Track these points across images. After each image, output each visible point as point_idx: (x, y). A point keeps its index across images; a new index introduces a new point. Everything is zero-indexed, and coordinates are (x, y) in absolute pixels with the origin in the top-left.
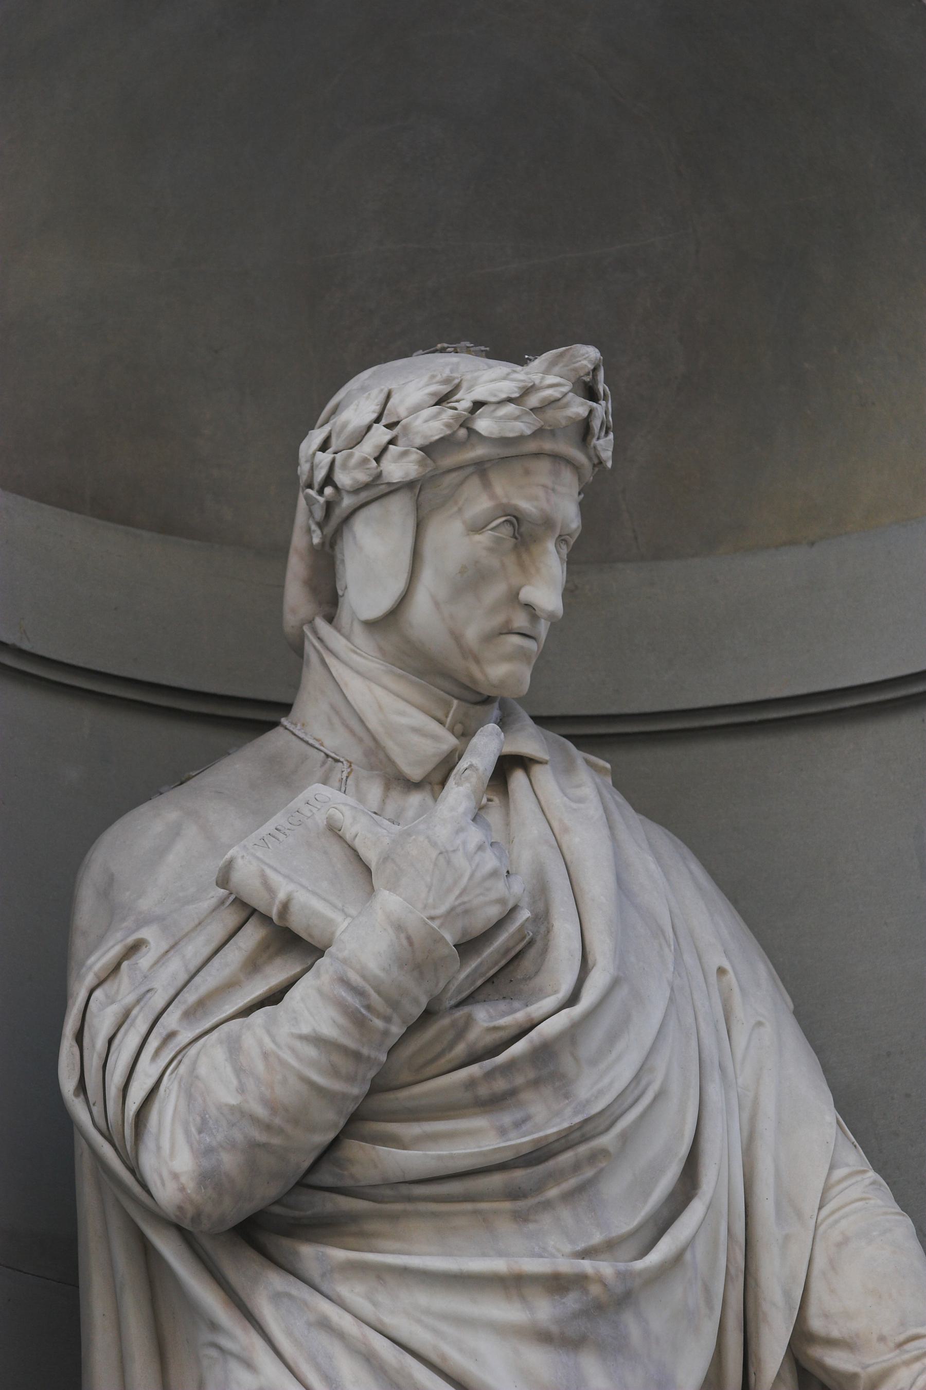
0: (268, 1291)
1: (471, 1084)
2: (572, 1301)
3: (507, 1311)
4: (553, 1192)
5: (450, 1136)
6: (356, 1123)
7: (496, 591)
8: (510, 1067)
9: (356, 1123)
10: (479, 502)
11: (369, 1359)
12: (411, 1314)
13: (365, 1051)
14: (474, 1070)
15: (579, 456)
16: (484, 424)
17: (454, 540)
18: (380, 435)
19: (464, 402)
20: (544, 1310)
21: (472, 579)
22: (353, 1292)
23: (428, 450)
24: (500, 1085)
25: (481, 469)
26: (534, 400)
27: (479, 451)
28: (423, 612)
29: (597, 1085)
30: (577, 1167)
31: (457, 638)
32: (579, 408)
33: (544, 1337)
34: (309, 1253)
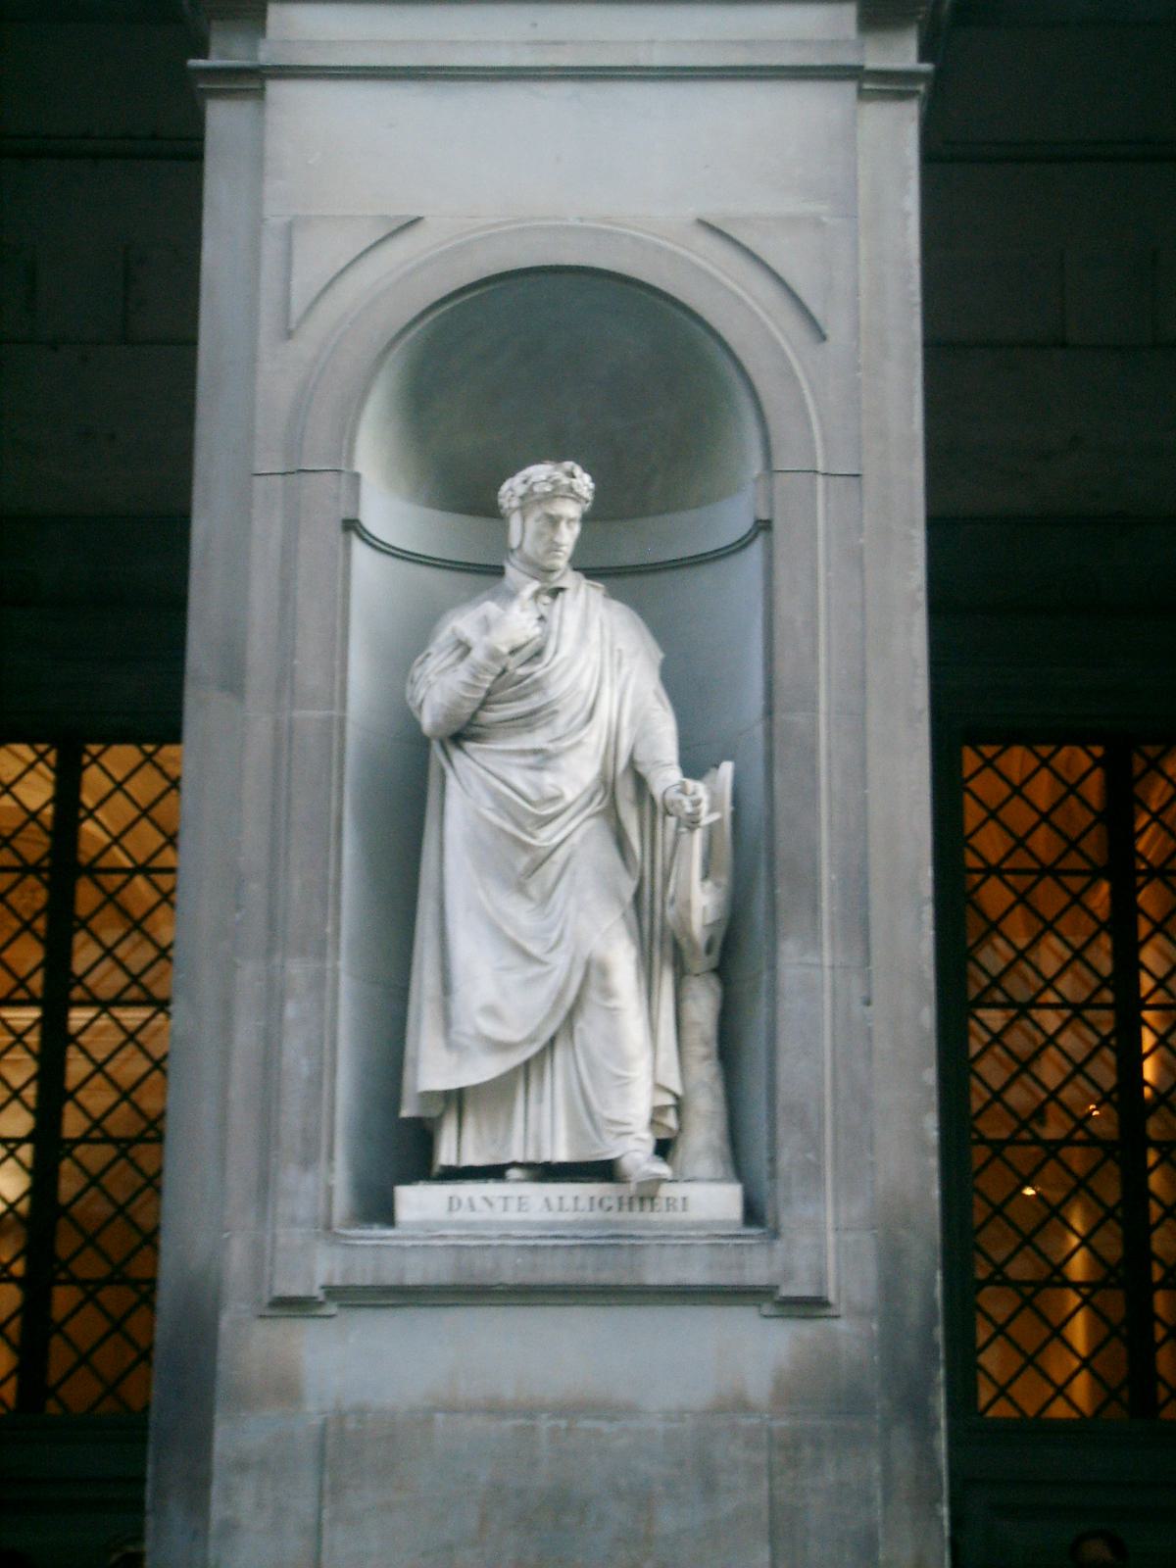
0: (457, 757)
1: (514, 693)
2: (540, 757)
3: (522, 761)
4: (540, 724)
5: (507, 709)
6: (484, 704)
7: (547, 538)
8: (526, 687)
9: (484, 704)
10: (537, 513)
11: (478, 775)
12: (493, 763)
13: (477, 684)
14: (514, 688)
15: (572, 495)
16: (536, 489)
17: (532, 525)
18: (510, 493)
19: (530, 483)
20: (531, 760)
21: (539, 535)
22: (477, 756)
23: (522, 498)
24: (524, 692)
25: (539, 502)
26: (551, 480)
27: (537, 497)
28: (528, 548)
29: (554, 692)
30: (548, 715)
31: (536, 553)
32: (566, 481)
33: (532, 768)
34: (470, 746)
